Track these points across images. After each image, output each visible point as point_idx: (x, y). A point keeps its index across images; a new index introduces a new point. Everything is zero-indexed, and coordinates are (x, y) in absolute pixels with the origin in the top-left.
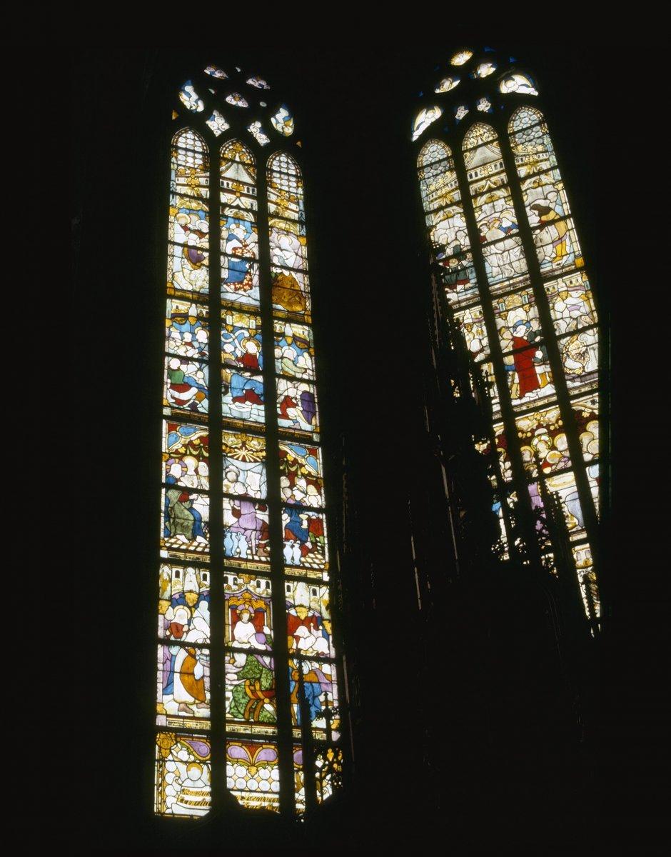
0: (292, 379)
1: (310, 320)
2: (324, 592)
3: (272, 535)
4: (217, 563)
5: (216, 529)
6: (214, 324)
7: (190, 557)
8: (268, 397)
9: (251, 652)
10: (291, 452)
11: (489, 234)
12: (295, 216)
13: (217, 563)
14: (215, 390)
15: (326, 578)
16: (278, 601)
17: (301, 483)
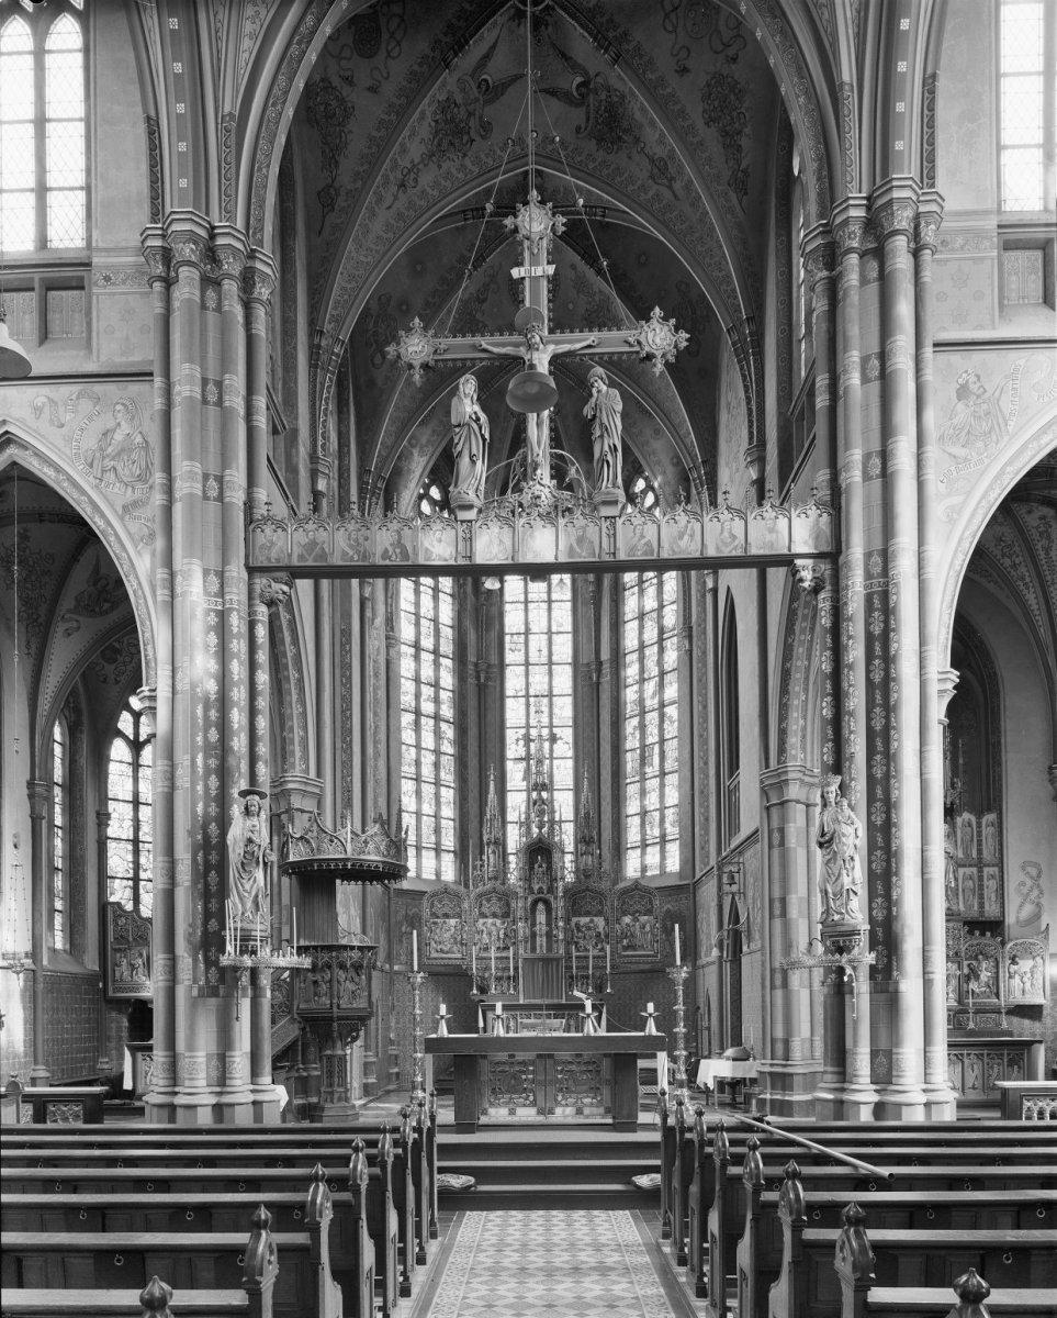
0: (444, 689)
1: (451, 656)
2: (452, 791)
3: (437, 765)
4: (418, 779)
5: (418, 763)
6: (417, 657)
7: (410, 776)
8: (437, 701)
9: (428, 815)
10: (444, 726)
11: (534, 628)
12: (448, 591)
13: (418, 779)
14: (418, 696)
15: (452, 785)
16: (437, 796)
17: (445, 741)
